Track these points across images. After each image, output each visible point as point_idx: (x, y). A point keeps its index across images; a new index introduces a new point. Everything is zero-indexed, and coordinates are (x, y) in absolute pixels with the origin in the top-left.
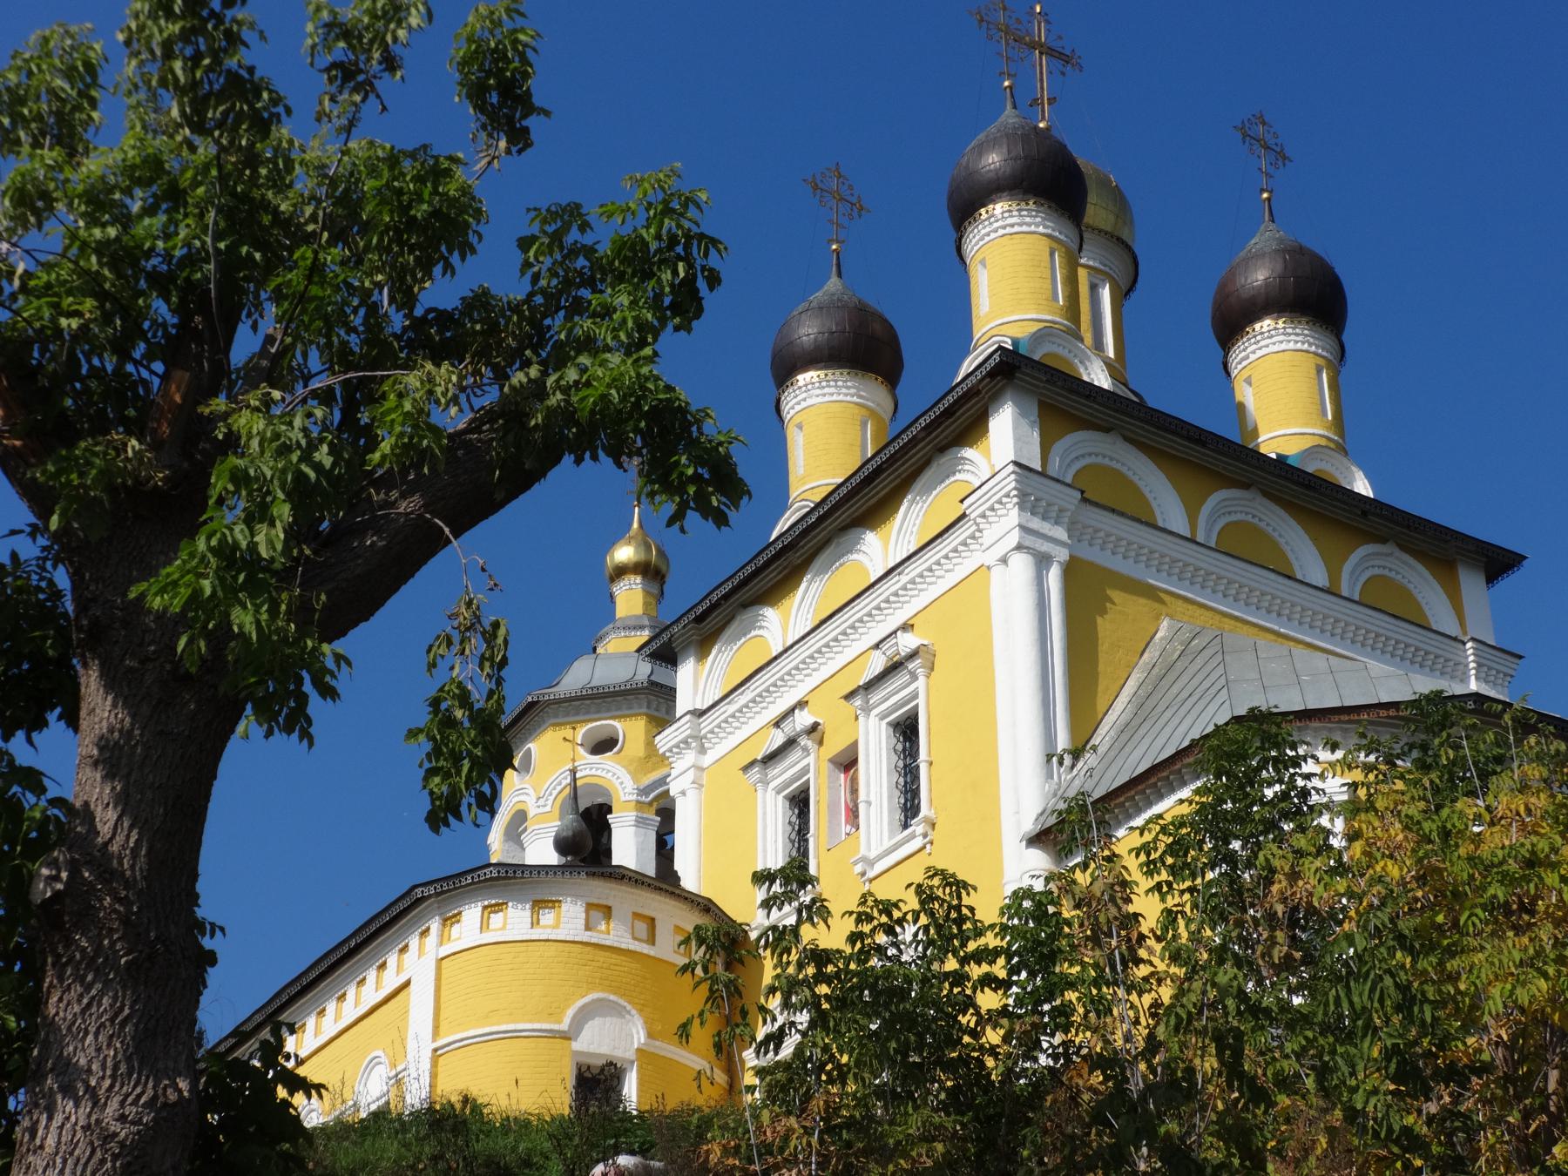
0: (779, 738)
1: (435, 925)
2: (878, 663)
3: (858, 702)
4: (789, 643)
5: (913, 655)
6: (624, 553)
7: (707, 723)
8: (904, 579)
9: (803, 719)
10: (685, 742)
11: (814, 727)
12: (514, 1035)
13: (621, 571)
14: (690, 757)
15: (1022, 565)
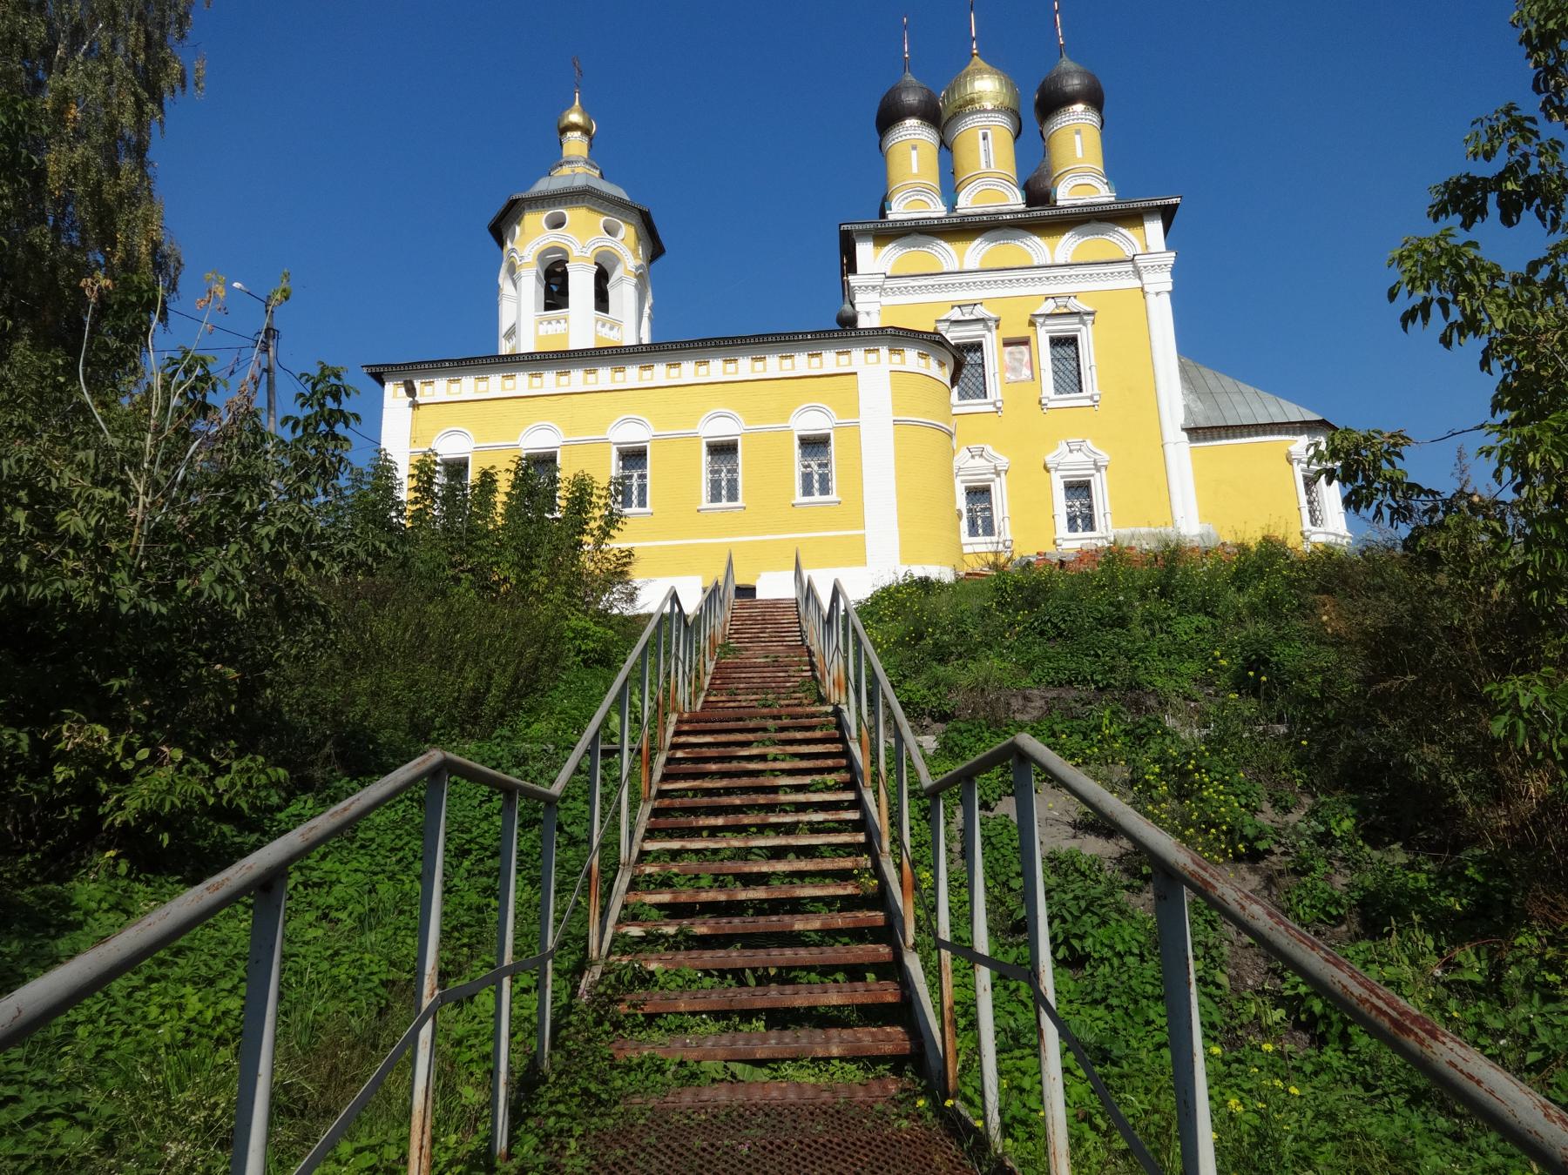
0: (956, 314)
1: (884, 351)
2: (1049, 307)
3: (1041, 320)
4: (966, 268)
5: (1089, 314)
6: (575, 117)
7: (890, 283)
8: (1072, 272)
9: (980, 312)
10: (874, 287)
11: (997, 321)
12: (938, 428)
13: (574, 127)
14: (874, 296)
15: (1167, 298)
